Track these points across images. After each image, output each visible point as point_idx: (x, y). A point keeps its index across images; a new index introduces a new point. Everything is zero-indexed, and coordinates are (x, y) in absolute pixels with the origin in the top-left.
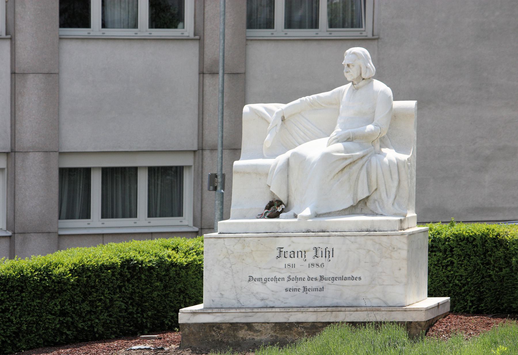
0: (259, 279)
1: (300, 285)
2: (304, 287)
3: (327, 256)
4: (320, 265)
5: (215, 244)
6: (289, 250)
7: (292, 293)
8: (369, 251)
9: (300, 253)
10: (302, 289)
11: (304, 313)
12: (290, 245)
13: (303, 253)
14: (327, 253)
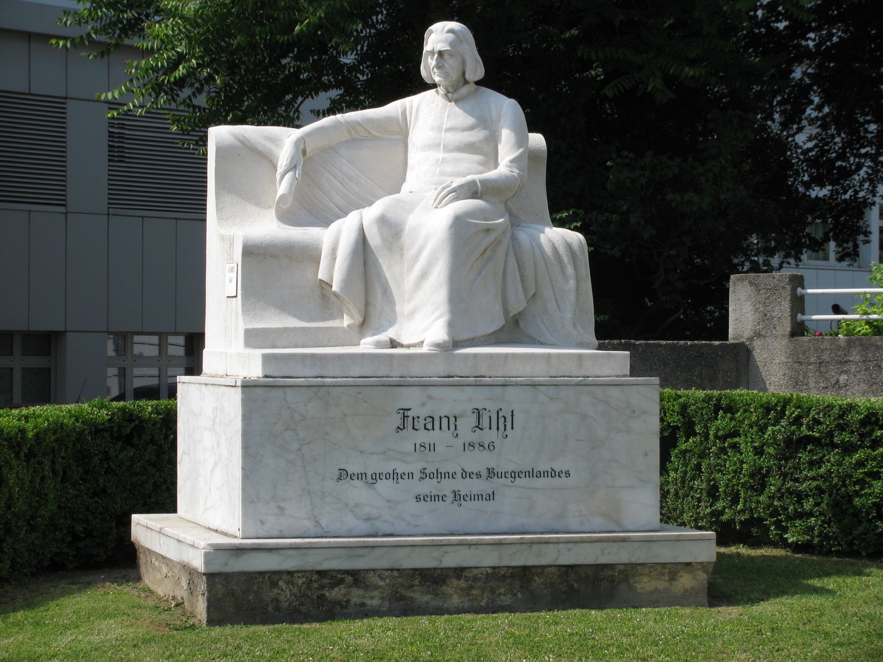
0: (361, 476)
2: (454, 492)
3: (501, 426)
4: (486, 446)
5: (265, 401)
6: (423, 413)
7: (429, 504)
9: (445, 422)
10: (450, 496)
11: (473, 547)
12: (423, 404)
13: (452, 421)
14: (501, 420)
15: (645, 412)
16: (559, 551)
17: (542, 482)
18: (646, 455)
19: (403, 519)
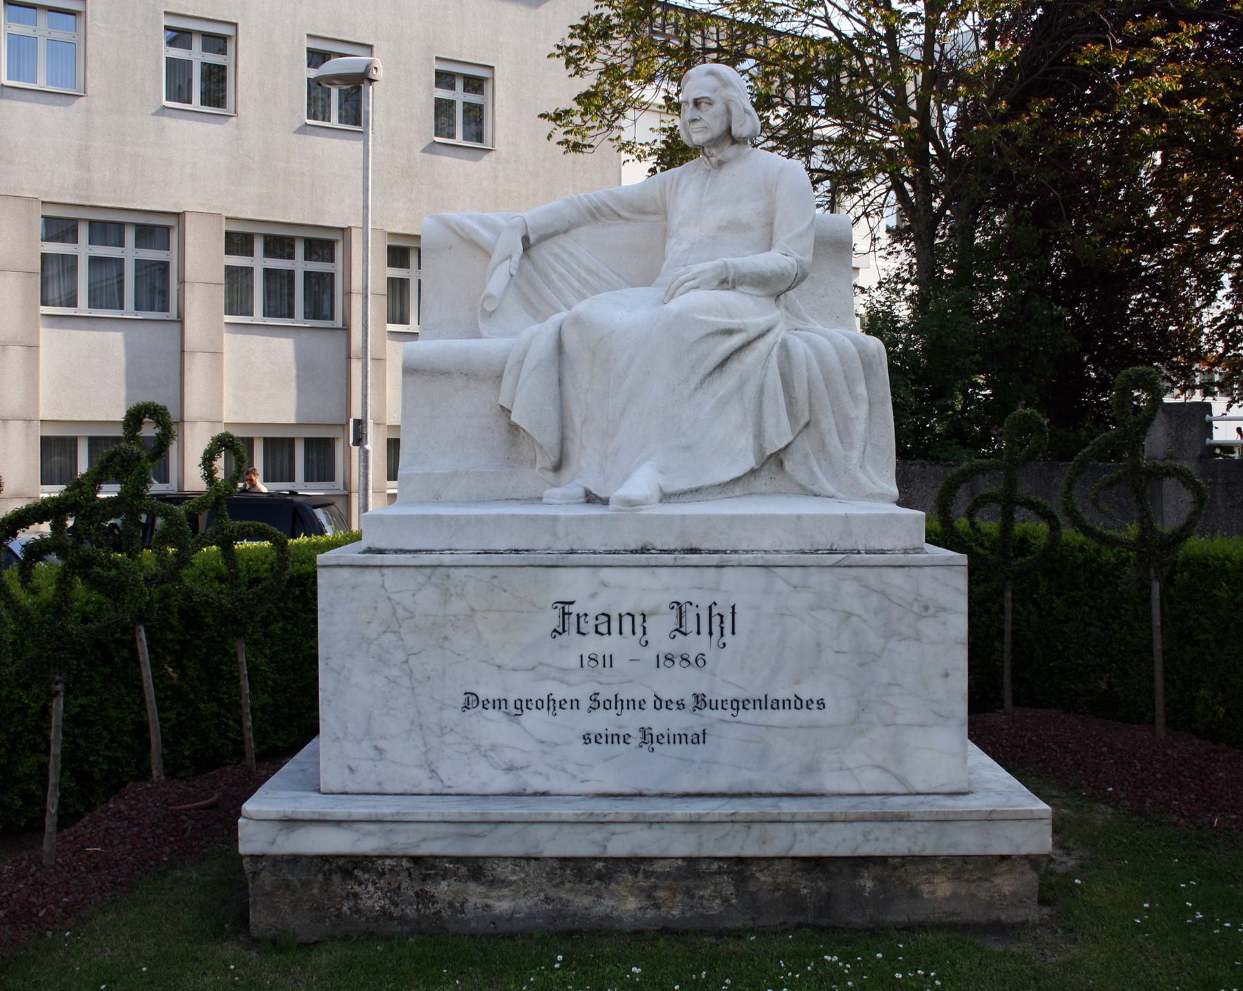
0: (499, 704)
1: (631, 721)
2: (643, 730)
3: (716, 630)
4: (692, 659)
5: (354, 588)
6: (593, 608)
8: (849, 615)
9: (627, 621)
10: (637, 737)
11: (655, 826)
12: (594, 595)
13: (638, 620)
14: (716, 620)
15: (944, 609)
16: (795, 835)
17: (780, 716)
18: (946, 675)
19: (564, 770)
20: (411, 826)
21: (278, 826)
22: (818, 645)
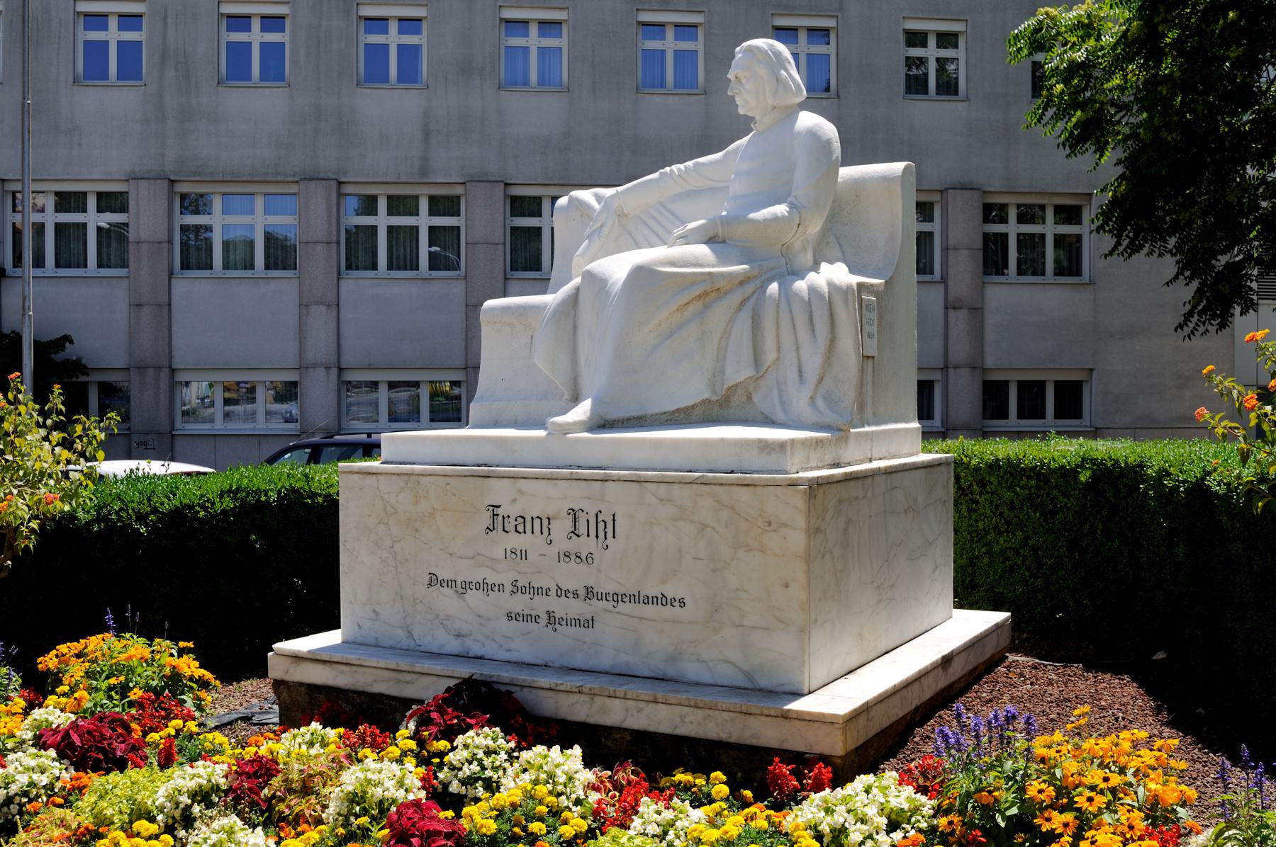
0: (451, 583)
1: (540, 605)
3: (601, 534)
4: (584, 557)
6: (514, 511)
7: (522, 625)
8: (705, 526)
9: (537, 522)
10: (544, 620)
12: (514, 500)
13: (545, 522)
14: (601, 525)
15: (785, 525)
16: (627, 710)
17: (650, 610)
18: (787, 586)
20: (367, 670)
21: (289, 661)
22: (680, 551)
